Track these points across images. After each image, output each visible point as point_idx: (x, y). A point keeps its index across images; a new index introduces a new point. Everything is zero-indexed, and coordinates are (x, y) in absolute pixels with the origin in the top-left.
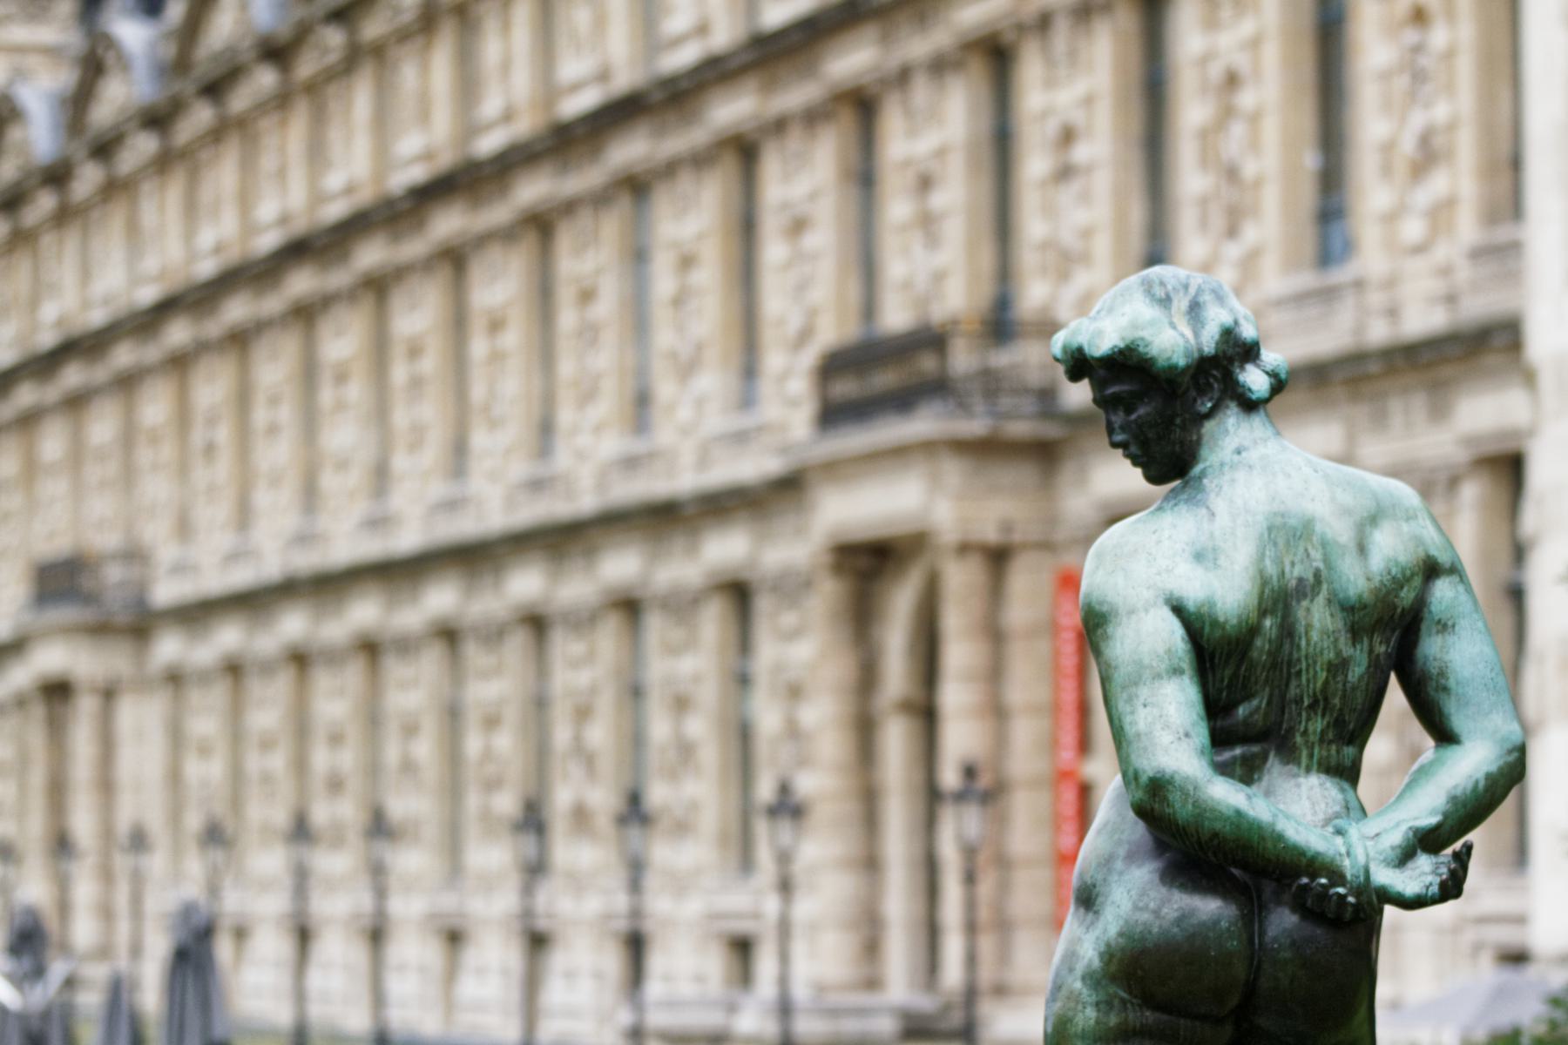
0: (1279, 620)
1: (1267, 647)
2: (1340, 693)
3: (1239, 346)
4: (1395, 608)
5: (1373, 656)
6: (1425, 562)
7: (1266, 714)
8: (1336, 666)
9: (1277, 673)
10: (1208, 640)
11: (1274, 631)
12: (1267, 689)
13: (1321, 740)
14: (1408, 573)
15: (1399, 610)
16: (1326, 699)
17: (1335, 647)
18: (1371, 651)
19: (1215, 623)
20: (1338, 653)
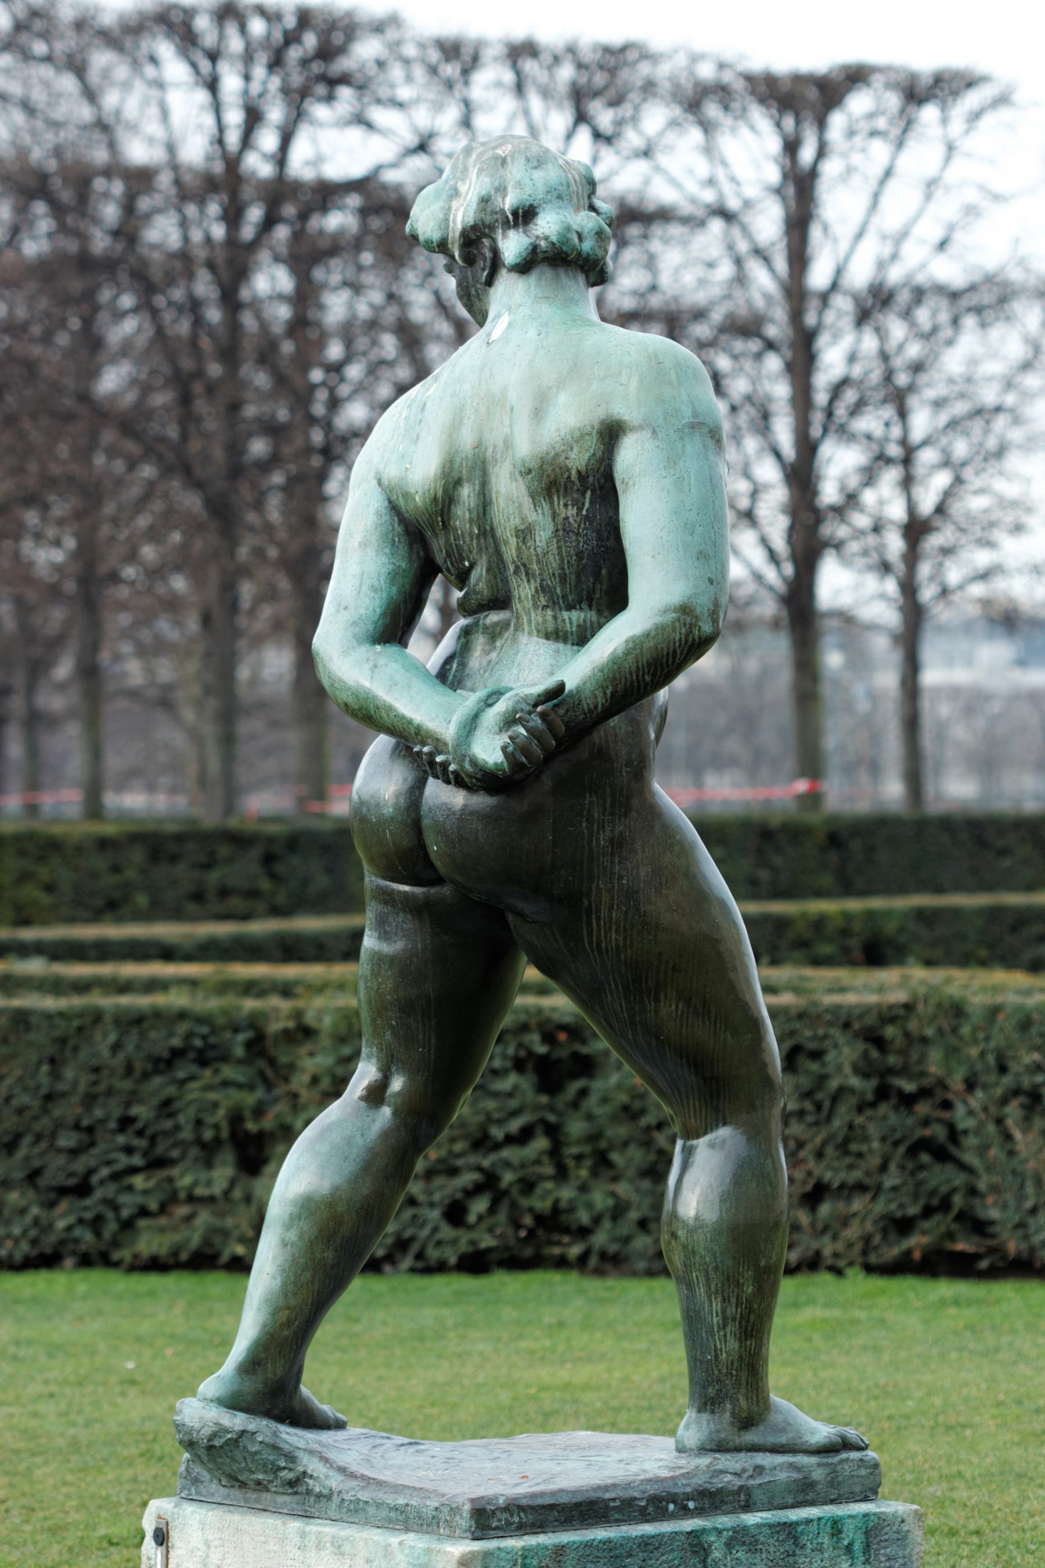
0: (477, 488)
1: (467, 515)
2: (535, 558)
3: (496, 213)
4: (568, 470)
5: (559, 520)
6: (603, 422)
7: (488, 582)
8: (523, 531)
9: (491, 540)
10: (407, 511)
11: (472, 499)
12: (484, 557)
13: (535, 606)
14: (577, 434)
15: (574, 472)
16: (525, 566)
17: (520, 512)
18: (554, 515)
19: (406, 495)
20: (523, 520)
